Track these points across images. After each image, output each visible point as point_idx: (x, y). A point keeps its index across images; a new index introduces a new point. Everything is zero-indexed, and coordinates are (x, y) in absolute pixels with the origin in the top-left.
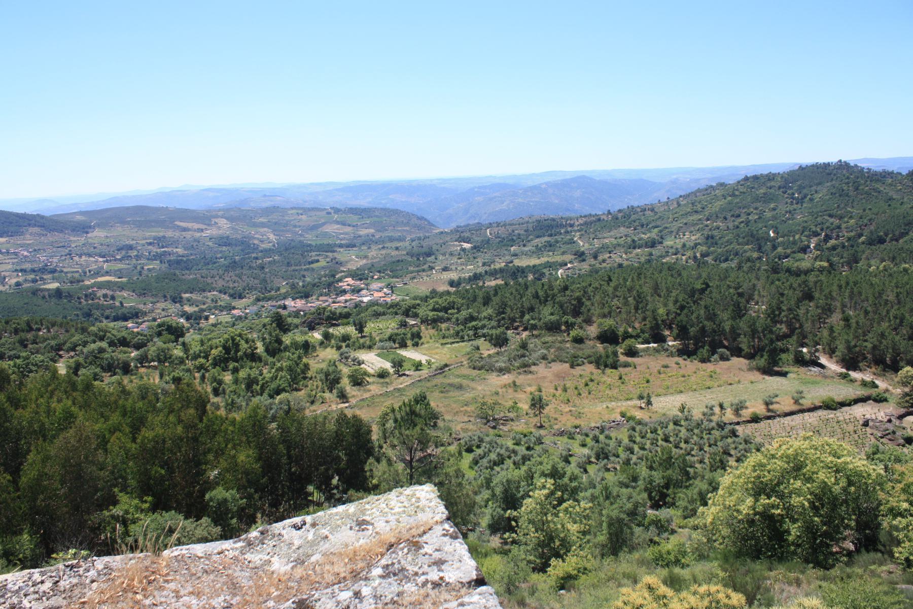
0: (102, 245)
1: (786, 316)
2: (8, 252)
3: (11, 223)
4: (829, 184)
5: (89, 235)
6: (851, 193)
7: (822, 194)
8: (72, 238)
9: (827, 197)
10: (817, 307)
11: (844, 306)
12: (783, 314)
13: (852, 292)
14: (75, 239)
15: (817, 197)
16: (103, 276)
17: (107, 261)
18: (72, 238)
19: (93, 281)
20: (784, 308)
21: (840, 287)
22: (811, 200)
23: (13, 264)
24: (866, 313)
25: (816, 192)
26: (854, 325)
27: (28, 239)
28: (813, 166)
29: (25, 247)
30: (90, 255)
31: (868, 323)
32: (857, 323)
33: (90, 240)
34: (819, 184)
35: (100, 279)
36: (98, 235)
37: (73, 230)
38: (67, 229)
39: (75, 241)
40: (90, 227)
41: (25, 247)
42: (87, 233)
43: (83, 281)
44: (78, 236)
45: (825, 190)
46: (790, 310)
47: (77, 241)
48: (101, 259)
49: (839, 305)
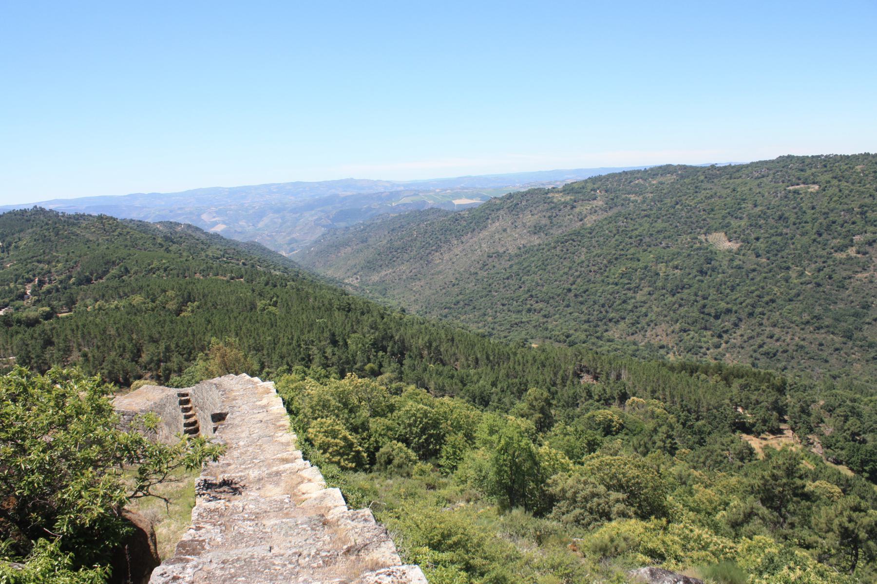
1: (36, 362)
4: (30, 231)
6: (53, 239)
7: (26, 240)
9: (32, 244)
10: (59, 350)
11: (79, 345)
12: (33, 361)
13: (83, 333)
15: (22, 244)
20: (33, 356)
21: (73, 330)
22: (17, 247)
24: (98, 347)
25: (20, 239)
26: (91, 359)
28: (10, 213)
31: (101, 355)
32: (94, 356)
34: (21, 231)
45: (28, 238)
46: (38, 356)
49: (75, 345)
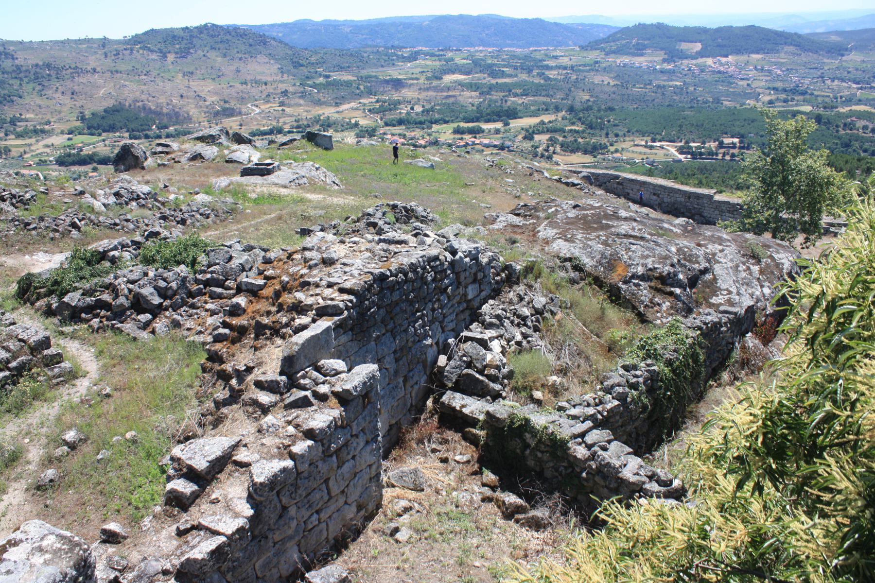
0: (857, 69)
2: (762, 70)
3: (769, 40)
5: (844, 58)
8: (825, 60)
14: (829, 61)
16: (858, 104)
17: (861, 88)
18: (825, 60)
19: (849, 108)
23: (766, 81)
27: (783, 58)
29: (779, 65)
30: (843, 80)
33: (844, 64)
35: (854, 108)
36: (854, 58)
37: (828, 52)
38: (822, 50)
39: (828, 64)
40: (846, 50)
41: (779, 65)
42: (843, 55)
43: (837, 107)
44: (832, 58)
47: (831, 63)
48: (855, 86)
